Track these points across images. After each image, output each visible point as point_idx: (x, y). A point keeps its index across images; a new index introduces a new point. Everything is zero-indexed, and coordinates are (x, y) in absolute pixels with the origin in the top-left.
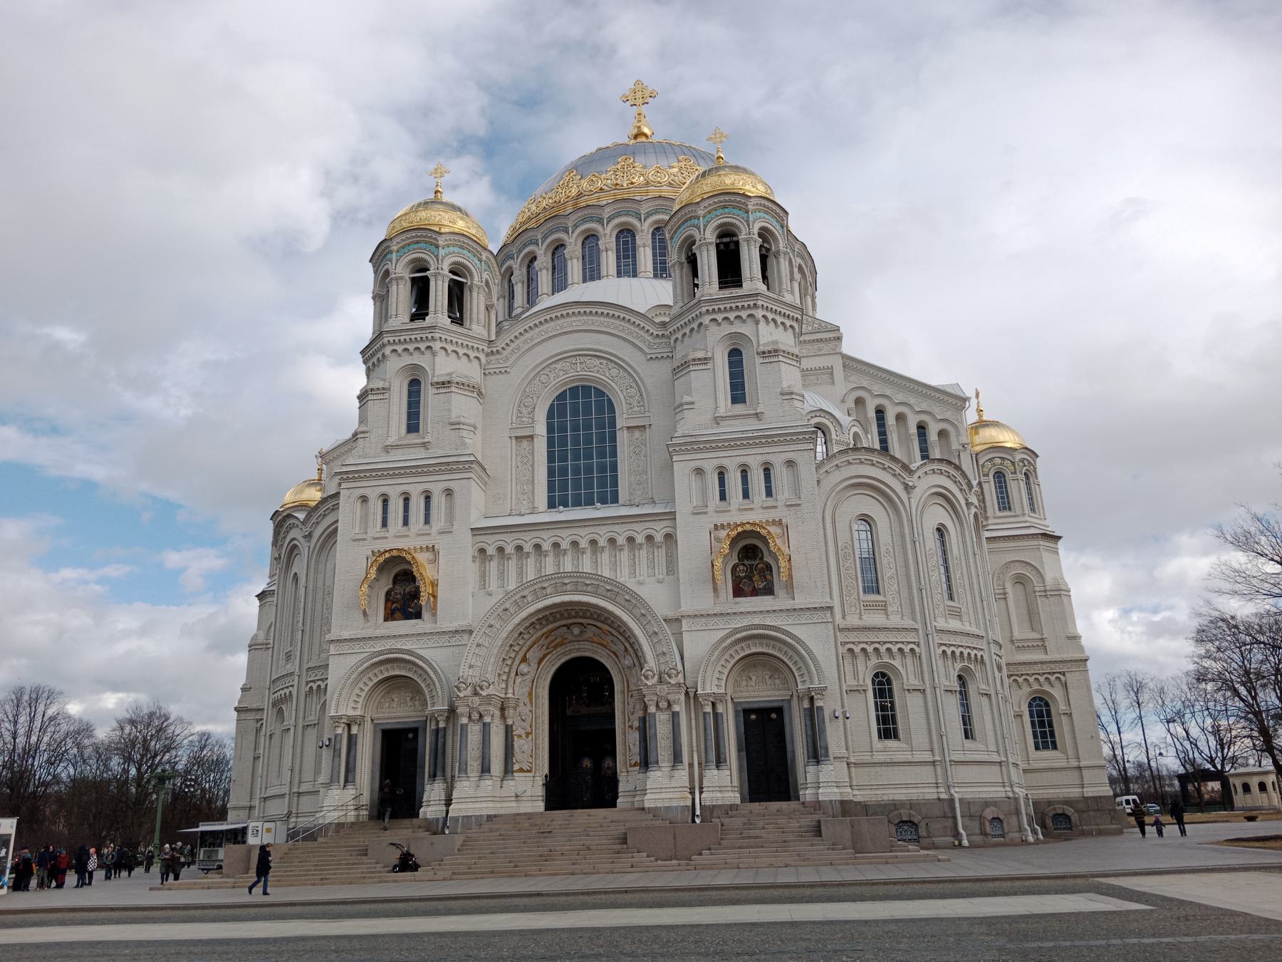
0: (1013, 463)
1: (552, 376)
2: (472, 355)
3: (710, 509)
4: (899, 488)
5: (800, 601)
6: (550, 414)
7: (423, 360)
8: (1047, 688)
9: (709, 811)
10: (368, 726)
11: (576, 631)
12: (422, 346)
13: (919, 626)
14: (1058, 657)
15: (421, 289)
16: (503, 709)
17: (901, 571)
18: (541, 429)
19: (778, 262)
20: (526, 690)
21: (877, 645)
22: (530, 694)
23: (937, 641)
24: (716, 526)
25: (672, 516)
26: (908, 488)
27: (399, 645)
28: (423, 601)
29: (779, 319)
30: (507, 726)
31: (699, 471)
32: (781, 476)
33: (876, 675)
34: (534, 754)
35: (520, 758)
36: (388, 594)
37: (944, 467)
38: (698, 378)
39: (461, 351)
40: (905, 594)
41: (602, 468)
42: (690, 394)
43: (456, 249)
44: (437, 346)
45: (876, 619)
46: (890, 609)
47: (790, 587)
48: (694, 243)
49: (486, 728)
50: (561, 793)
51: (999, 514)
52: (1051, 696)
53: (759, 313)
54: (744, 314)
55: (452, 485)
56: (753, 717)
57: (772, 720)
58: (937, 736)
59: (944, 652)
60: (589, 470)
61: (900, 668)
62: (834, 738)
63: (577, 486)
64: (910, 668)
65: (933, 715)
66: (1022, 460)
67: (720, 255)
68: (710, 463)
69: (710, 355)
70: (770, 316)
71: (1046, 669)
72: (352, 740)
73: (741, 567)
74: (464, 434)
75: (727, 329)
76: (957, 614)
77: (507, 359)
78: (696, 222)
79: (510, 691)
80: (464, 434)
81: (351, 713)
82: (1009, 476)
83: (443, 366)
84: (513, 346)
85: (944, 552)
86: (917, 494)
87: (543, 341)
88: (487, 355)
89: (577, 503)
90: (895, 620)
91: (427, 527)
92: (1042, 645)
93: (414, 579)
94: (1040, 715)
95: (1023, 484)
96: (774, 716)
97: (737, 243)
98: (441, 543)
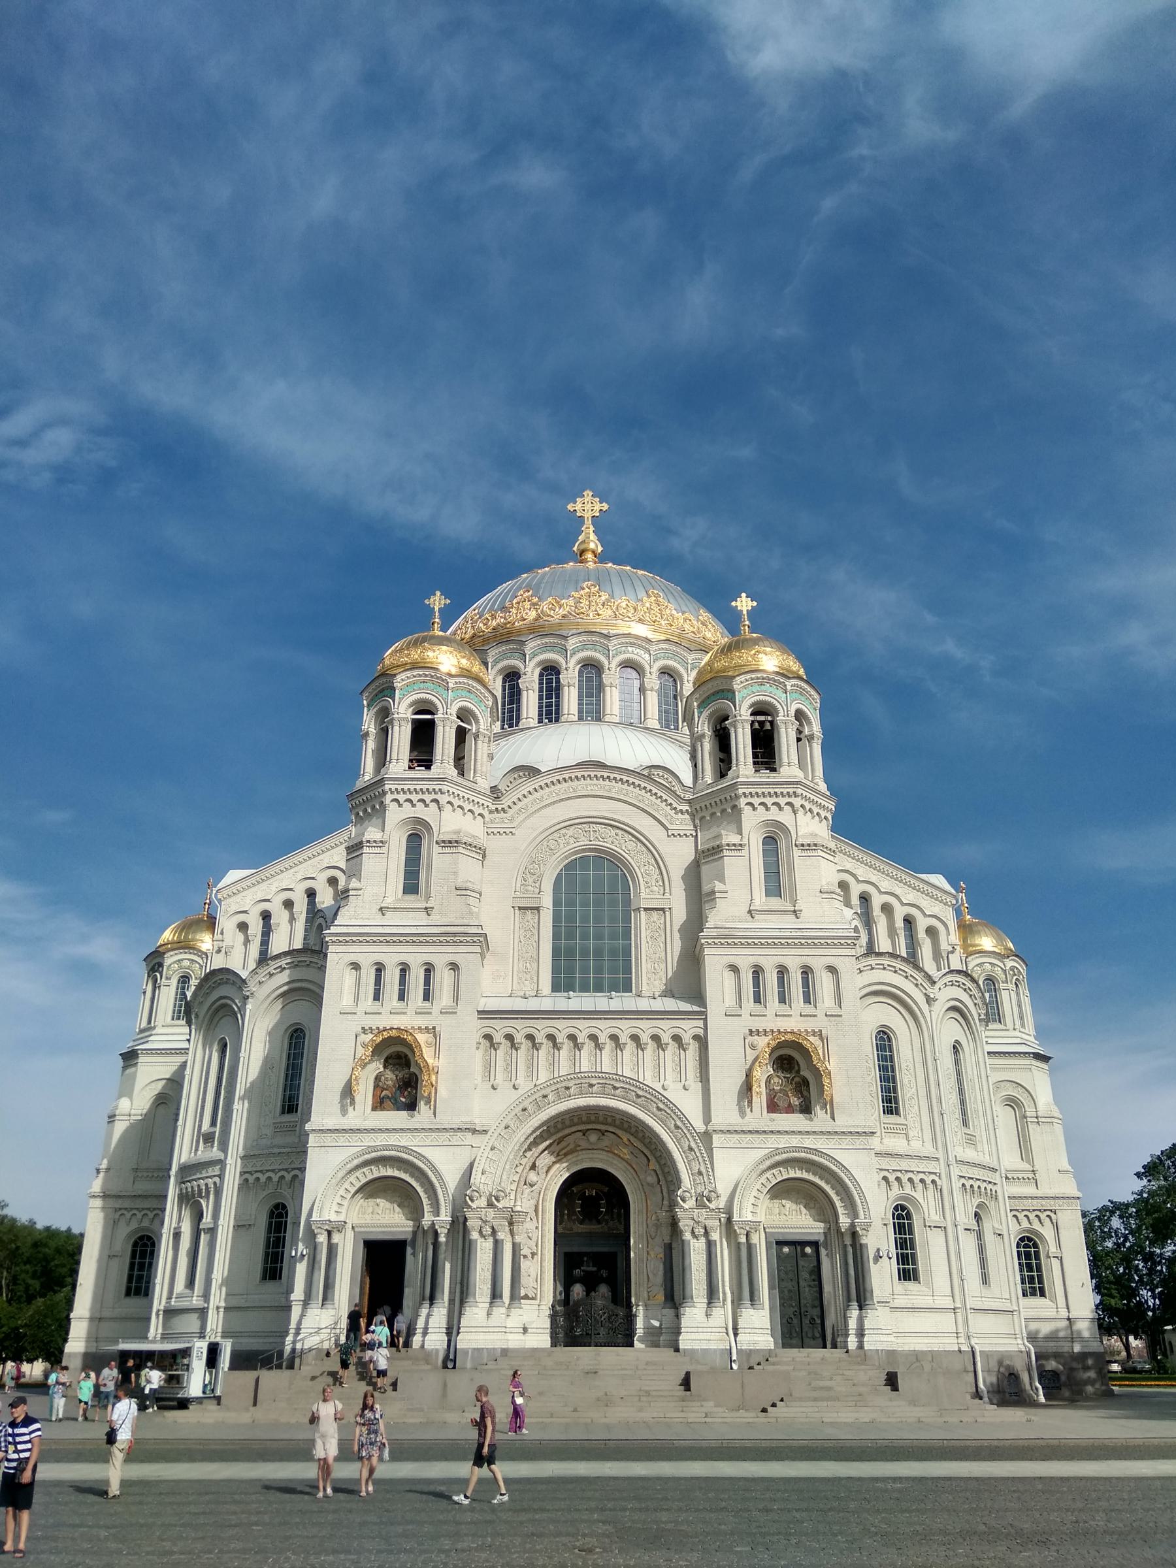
0: (1004, 971)
1: (561, 842)
2: (477, 810)
3: (745, 1012)
4: (921, 1000)
5: (843, 1122)
7: (428, 814)
8: (1036, 1226)
9: (746, 1354)
10: (350, 1235)
11: (593, 1138)
12: (428, 798)
13: (940, 1155)
14: (1050, 1193)
15: (423, 734)
16: (511, 1224)
17: (922, 1092)
18: (547, 901)
19: (811, 746)
20: (533, 1202)
21: (899, 1174)
22: (536, 1207)
24: (751, 1031)
25: (703, 1015)
26: (929, 1000)
28: (424, 1091)
29: (816, 810)
30: (514, 1244)
31: (734, 969)
32: (824, 984)
33: (896, 1208)
34: (540, 1279)
35: (528, 1283)
36: (378, 1078)
37: (961, 979)
38: (732, 864)
39: (467, 806)
41: (614, 952)
43: (464, 693)
44: (443, 799)
46: (911, 1134)
47: (829, 1106)
48: (727, 718)
49: (497, 1245)
53: (797, 802)
55: (456, 959)
56: (786, 1250)
57: (804, 1254)
59: (963, 1185)
60: (599, 952)
61: (921, 1201)
63: (585, 970)
64: (931, 1200)
65: (952, 1255)
66: (1012, 969)
67: (755, 734)
68: (745, 959)
69: (745, 841)
70: (808, 806)
71: (1036, 1204)
72: (332, 1250)
73: (776, 1080)
74: (471, 901)
75: (762, 815)
77: (512, 820)
78: (730, 695)
79: (519, 1203)
80: (471, 901)
81: (333, 1217)
83: (449, 822)
84: (520, 804)
85: (959, 1073)
87: (554, 803)
88: (491, 812)
89: (585, 988)
90: (916, 1147)
91: (427, 1004)
92: (1033, 1177)
93: (408, 1064)
94: (1028, 1256)
96: (808, 1250)
97: (772, 723)
98: (444, 1025)
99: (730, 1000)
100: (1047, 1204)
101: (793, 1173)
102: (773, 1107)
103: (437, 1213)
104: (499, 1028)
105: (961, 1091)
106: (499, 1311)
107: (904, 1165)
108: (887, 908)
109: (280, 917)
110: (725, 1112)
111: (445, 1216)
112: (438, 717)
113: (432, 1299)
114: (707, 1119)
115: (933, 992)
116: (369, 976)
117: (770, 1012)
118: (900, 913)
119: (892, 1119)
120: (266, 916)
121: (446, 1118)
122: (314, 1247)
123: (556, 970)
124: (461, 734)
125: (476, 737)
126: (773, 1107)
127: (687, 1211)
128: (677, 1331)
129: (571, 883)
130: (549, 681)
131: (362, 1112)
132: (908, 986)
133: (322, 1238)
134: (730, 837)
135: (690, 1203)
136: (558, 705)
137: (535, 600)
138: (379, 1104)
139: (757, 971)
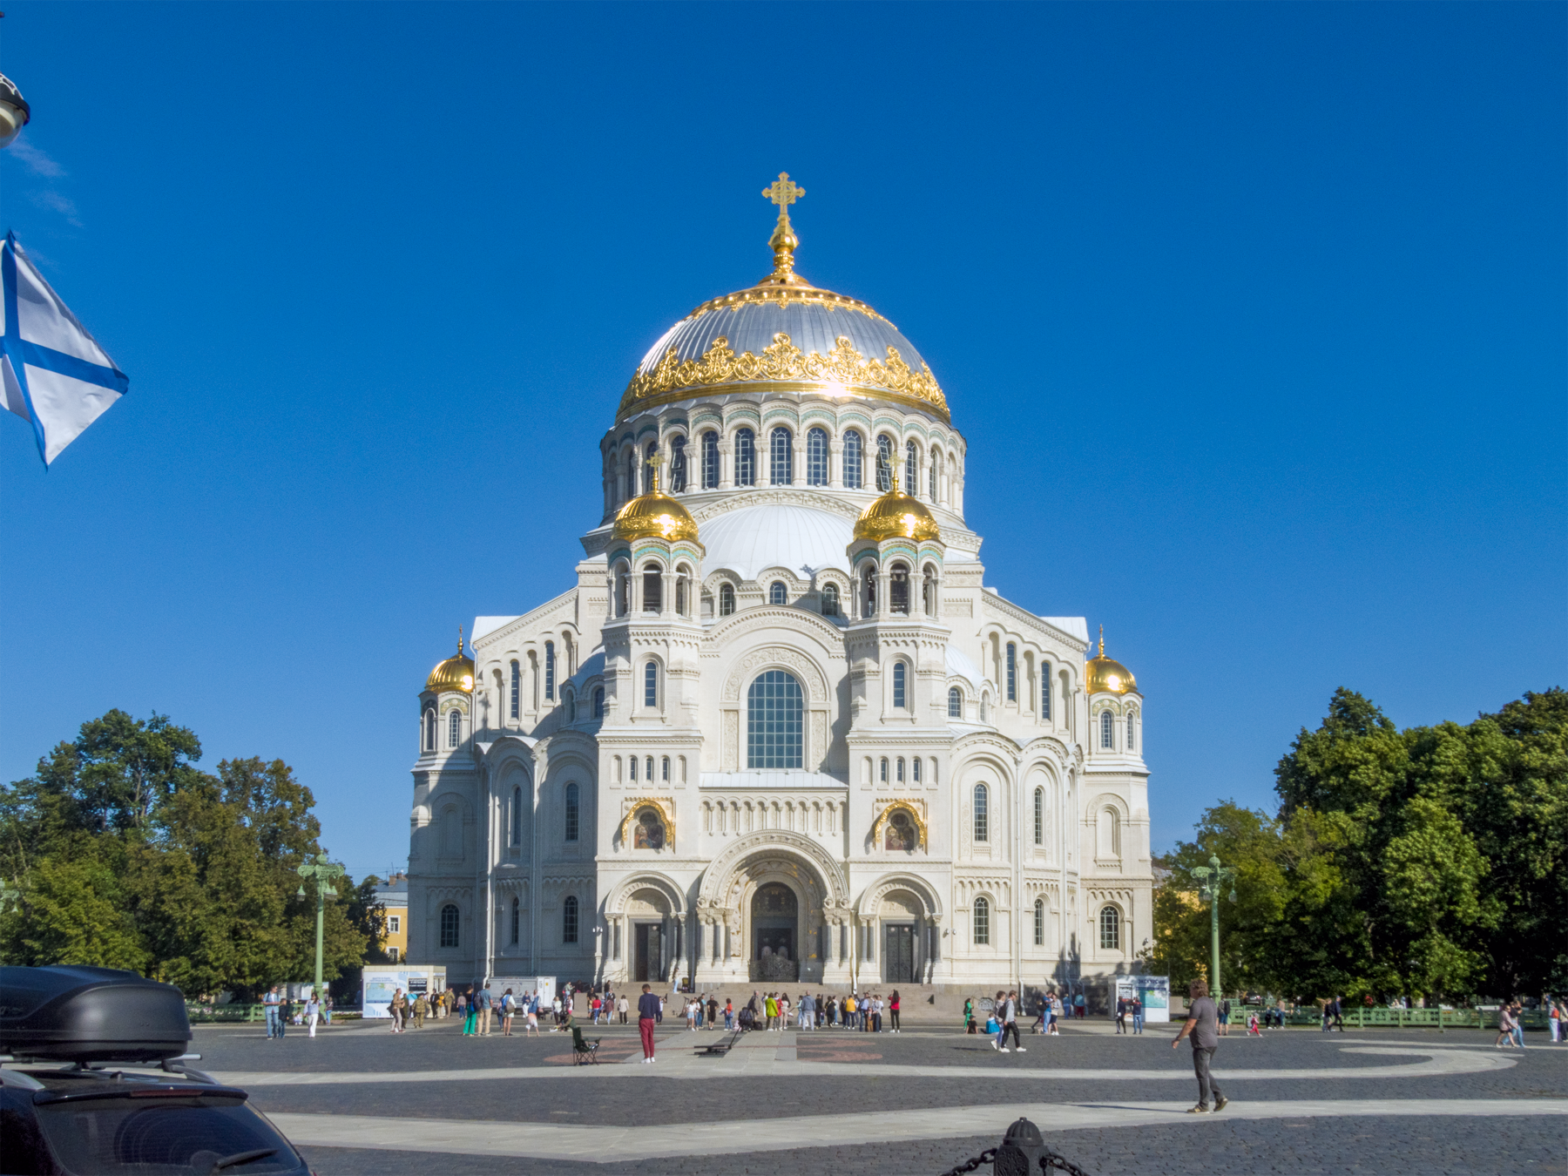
3: (874, 788)
5: (932, 856)
6: (751, 693)
7: (660, 650)
8: (1117, 899)
13: (1013, 867)
15: (653, 586)
17: (1005, 824)
23: (1024, 874)
26: (1016, 762)
27: (650, 867)
31: (869, 759)
35: (735, 948)
38: (871, 684)
40: (1005, 842)
42: (864, 696)
44: (670, 639)
45: (982, 860)
50: (761, 971)
51: (1101, 750)
52: (1120, 907)
54: (908, 639)
55: (684, 753)
58: (1014, 941)
60: (780, 739)
62: (944, 945)
63: (770, 752)
68: (877, 753)
71: (1119, 884)
72: (617, 929)
76: (1041, 854)
82: (1116, 718)
83: (675, 655)
86: (1021, 766)
92: (1119, 865)
94: (1109, 920)
95: (1125, 725)
99: (865, 779)
100: (1126, 884)
101: (898, 887)
102: (889, 846)
103: (678, 908)
104: (714, 798)
105: (1038, 820)
106: (719, 963)
107: (985, 873)
108: (1029, 655)
109: (526, 665)
110: (857, 850)
111: (683, 912)
112: (664, 574)
113: (679, 957)
114: (847, 854)
115: (1019, 756)
116: (627, 764)
117: (890, 788)
118: (1038, 659)
119: (982, 843)
120: (515, 664)
121: (680, 855)
122: (606, 928)
123: (751, 752)
124: (680, 583)
125: (690, 582)
126: (889, 846)
127: (830, 908)
128: (822, 974)
129: (760, 693)
130: (744, 444)
131: (628, 849)
132: (1002, 753)
133: (611, 923)
134: (869, 664)
135: (832, 906)
136: (752, 467)
137: (731, 354)
138: (639, 844)
139: (885, 761)
